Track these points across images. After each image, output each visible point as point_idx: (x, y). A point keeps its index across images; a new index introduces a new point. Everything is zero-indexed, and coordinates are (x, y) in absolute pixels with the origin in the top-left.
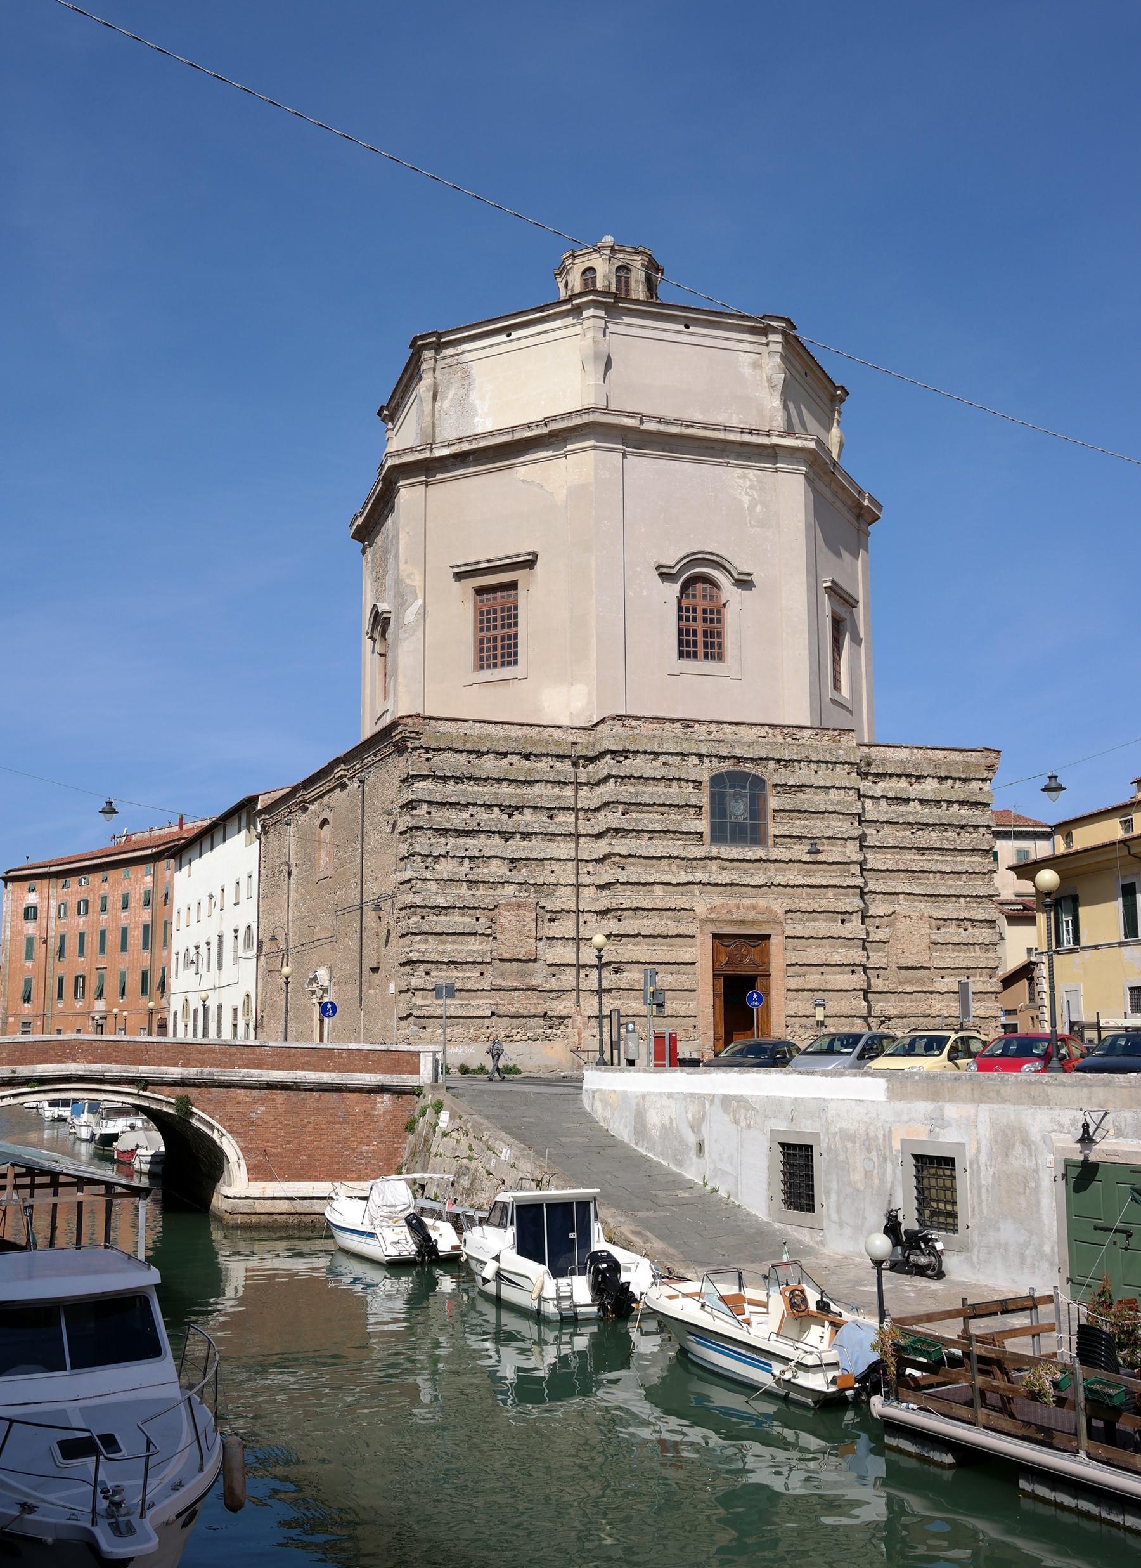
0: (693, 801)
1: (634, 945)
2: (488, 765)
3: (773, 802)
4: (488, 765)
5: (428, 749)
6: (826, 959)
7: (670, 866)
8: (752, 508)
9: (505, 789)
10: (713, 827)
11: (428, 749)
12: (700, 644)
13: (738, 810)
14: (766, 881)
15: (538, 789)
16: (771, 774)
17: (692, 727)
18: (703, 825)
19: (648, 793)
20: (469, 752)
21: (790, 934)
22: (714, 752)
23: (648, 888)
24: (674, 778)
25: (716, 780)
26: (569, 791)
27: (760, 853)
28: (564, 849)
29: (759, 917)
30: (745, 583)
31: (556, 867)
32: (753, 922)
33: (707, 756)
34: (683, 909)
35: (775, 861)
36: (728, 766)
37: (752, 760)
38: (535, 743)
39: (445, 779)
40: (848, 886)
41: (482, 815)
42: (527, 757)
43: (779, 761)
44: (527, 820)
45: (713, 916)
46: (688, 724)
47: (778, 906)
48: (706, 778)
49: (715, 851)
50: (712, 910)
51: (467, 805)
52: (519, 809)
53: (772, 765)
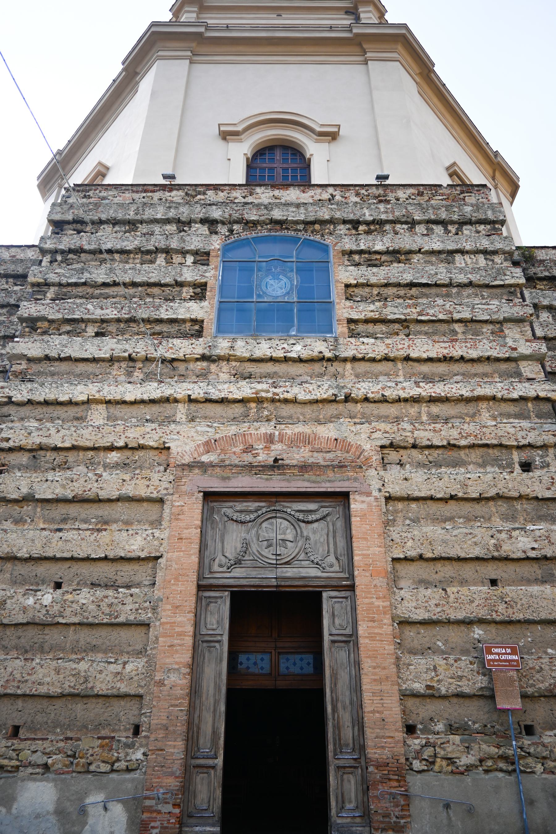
1: (18, 521)
6: (497, 547)
7: (129, 374)
14: (335, 391)
17: (204, 194)
21: (396, 489)
22: (236, 216)
23: (72, 411)
24: (157, 251)
29: (319, 458)
32: (304, 468)
33: (223, 223)
34: (141, 447)
40: (523, 399)
45: (205, 458)
50: (208, 446)
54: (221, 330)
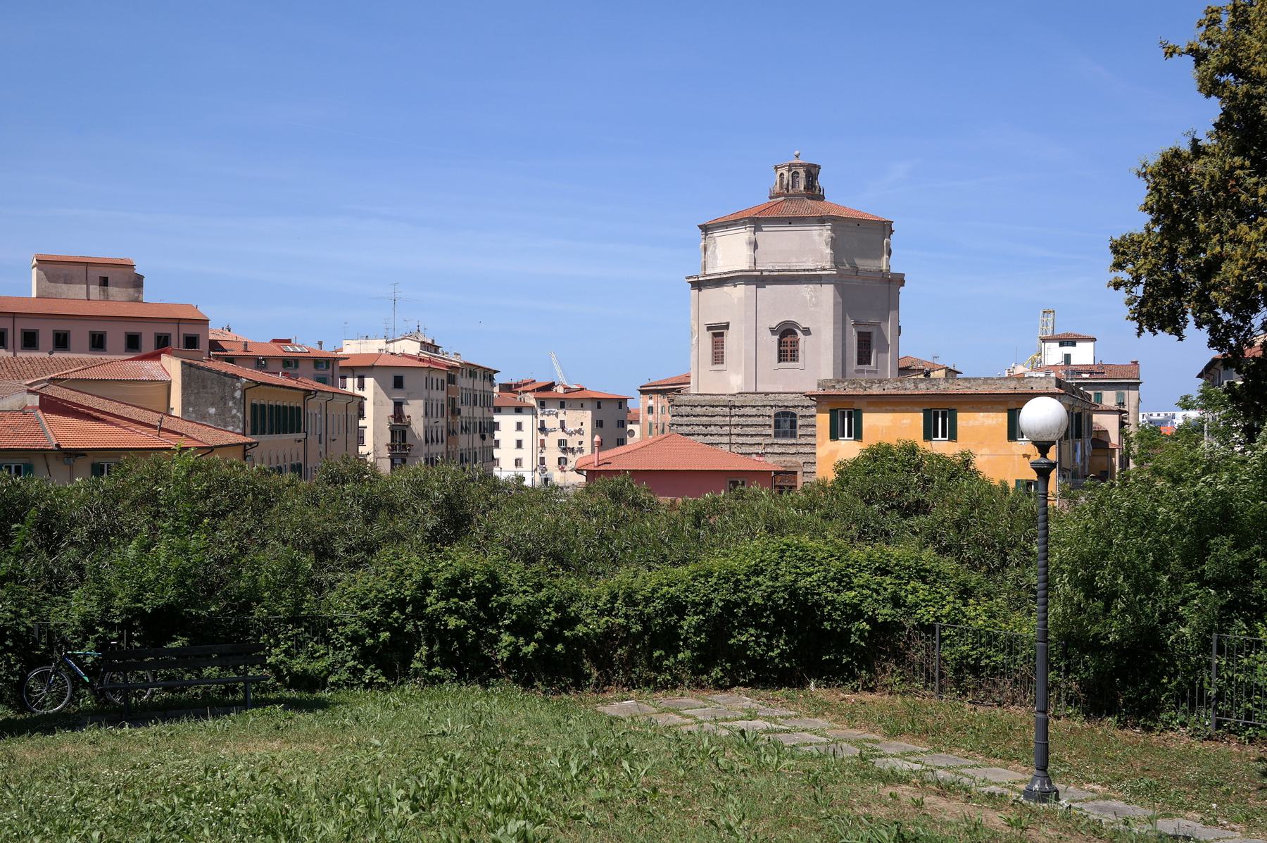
0: (768, 423)
2: (698, 410)
3: (799, 422)
4: (698, 410)
5: (676, 406)
8: (810, 300)
9: (705, 419)
10: (775, 433)
11: (676, 406)
12: (789, 356)
13: (786, 426)
15: (716, 418)
16: (799, 412)
18: (771, 431)
19: (750, 421)
20: (691, 406)
25: (776, 415)
26: (728, 419)
27: (793, 441)
28: (726, 440)
30: (807, 332)
31: (723, 446)
35: (800, 444)
36: (782, 409)
37: (792, 407)
38: (715, 401)
39: (682, 416)
41: (696, 428)
42: (713, 406)
43: (803, 406)
44: (712, 429)
46: (766, 394)
47: (801, 460)
48: (773, 414)
49: (776, 441)
51: (690, 425)
52: (710, 426)
53: (800, 408)
54: (775, 437)
